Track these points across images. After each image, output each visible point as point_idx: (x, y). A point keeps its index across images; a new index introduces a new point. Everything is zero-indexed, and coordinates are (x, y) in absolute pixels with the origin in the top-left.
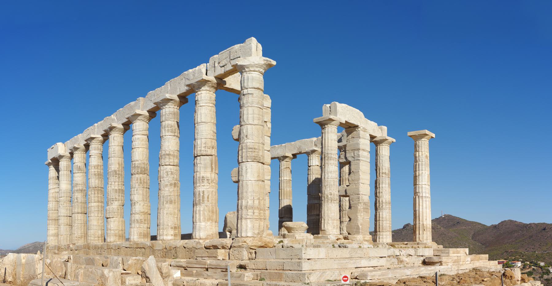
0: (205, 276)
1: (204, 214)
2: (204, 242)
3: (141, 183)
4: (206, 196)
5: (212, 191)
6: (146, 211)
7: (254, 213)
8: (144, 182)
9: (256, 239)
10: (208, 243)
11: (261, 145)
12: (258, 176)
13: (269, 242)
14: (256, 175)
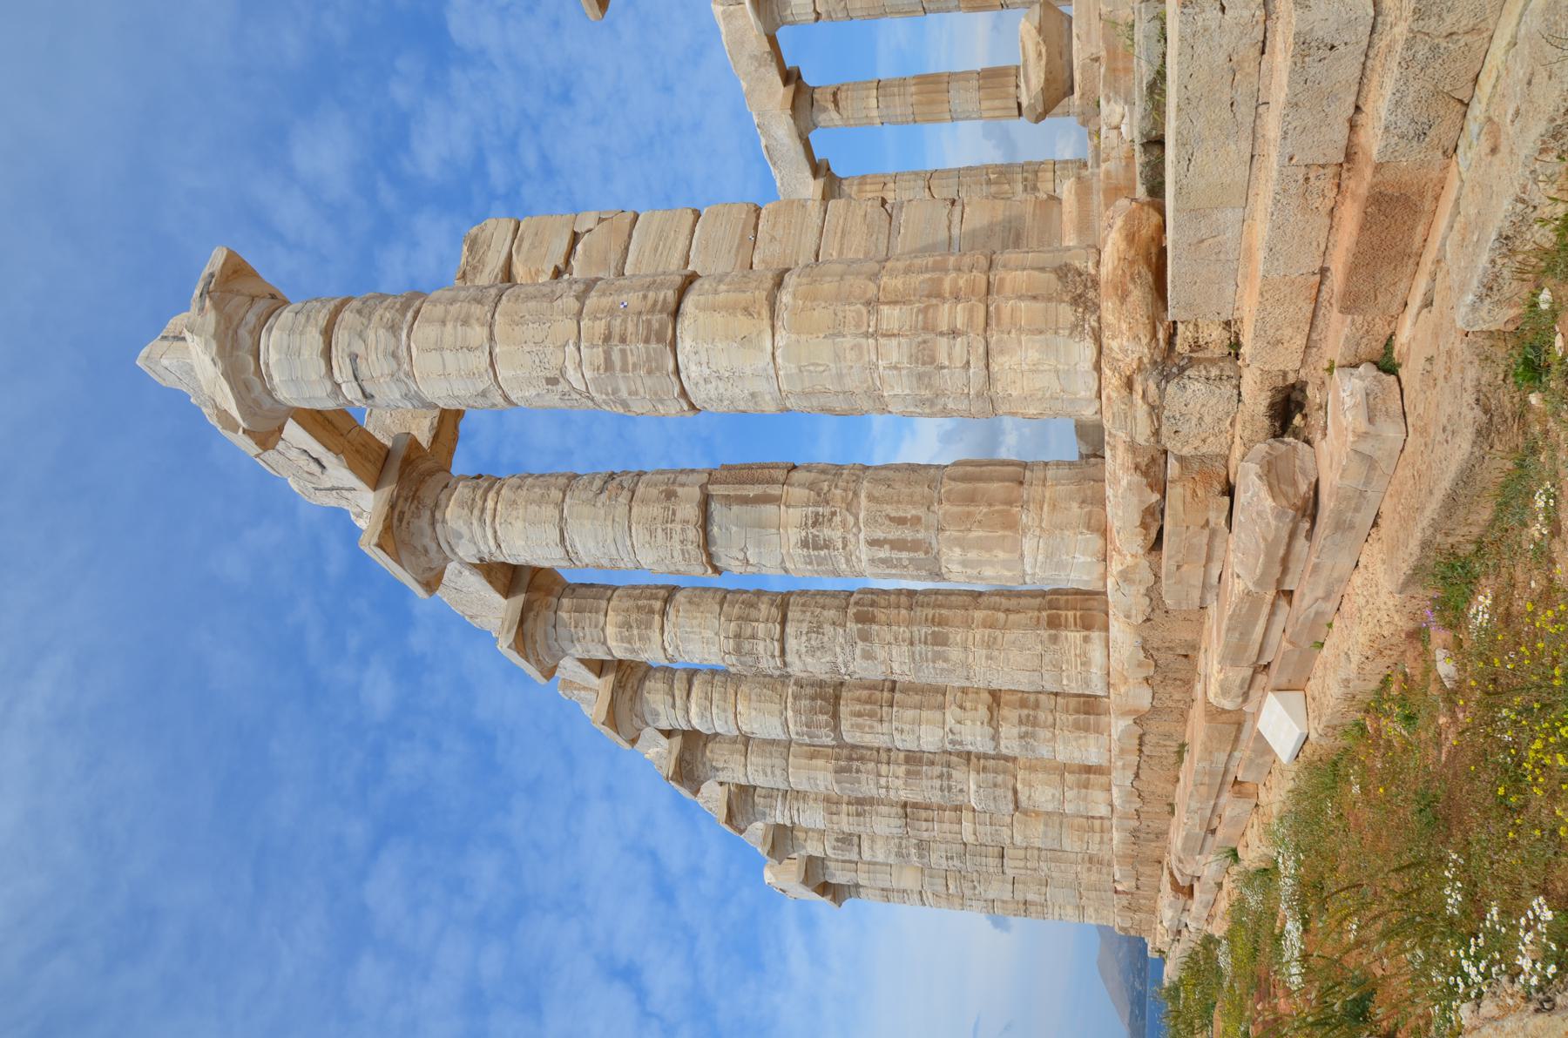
0: (1330, 607)
1: (980, 544)
2: (1119, 553)
3: (871, 715)
4: (896, 533)
5: (871, 498)
6: (986, 696)
7: (954, 333)
8: (869, 701)
9: (1109, 317)
10: (1128, 544)
11: (592, 301)
13: (1131, 238)
14: (742, 323)
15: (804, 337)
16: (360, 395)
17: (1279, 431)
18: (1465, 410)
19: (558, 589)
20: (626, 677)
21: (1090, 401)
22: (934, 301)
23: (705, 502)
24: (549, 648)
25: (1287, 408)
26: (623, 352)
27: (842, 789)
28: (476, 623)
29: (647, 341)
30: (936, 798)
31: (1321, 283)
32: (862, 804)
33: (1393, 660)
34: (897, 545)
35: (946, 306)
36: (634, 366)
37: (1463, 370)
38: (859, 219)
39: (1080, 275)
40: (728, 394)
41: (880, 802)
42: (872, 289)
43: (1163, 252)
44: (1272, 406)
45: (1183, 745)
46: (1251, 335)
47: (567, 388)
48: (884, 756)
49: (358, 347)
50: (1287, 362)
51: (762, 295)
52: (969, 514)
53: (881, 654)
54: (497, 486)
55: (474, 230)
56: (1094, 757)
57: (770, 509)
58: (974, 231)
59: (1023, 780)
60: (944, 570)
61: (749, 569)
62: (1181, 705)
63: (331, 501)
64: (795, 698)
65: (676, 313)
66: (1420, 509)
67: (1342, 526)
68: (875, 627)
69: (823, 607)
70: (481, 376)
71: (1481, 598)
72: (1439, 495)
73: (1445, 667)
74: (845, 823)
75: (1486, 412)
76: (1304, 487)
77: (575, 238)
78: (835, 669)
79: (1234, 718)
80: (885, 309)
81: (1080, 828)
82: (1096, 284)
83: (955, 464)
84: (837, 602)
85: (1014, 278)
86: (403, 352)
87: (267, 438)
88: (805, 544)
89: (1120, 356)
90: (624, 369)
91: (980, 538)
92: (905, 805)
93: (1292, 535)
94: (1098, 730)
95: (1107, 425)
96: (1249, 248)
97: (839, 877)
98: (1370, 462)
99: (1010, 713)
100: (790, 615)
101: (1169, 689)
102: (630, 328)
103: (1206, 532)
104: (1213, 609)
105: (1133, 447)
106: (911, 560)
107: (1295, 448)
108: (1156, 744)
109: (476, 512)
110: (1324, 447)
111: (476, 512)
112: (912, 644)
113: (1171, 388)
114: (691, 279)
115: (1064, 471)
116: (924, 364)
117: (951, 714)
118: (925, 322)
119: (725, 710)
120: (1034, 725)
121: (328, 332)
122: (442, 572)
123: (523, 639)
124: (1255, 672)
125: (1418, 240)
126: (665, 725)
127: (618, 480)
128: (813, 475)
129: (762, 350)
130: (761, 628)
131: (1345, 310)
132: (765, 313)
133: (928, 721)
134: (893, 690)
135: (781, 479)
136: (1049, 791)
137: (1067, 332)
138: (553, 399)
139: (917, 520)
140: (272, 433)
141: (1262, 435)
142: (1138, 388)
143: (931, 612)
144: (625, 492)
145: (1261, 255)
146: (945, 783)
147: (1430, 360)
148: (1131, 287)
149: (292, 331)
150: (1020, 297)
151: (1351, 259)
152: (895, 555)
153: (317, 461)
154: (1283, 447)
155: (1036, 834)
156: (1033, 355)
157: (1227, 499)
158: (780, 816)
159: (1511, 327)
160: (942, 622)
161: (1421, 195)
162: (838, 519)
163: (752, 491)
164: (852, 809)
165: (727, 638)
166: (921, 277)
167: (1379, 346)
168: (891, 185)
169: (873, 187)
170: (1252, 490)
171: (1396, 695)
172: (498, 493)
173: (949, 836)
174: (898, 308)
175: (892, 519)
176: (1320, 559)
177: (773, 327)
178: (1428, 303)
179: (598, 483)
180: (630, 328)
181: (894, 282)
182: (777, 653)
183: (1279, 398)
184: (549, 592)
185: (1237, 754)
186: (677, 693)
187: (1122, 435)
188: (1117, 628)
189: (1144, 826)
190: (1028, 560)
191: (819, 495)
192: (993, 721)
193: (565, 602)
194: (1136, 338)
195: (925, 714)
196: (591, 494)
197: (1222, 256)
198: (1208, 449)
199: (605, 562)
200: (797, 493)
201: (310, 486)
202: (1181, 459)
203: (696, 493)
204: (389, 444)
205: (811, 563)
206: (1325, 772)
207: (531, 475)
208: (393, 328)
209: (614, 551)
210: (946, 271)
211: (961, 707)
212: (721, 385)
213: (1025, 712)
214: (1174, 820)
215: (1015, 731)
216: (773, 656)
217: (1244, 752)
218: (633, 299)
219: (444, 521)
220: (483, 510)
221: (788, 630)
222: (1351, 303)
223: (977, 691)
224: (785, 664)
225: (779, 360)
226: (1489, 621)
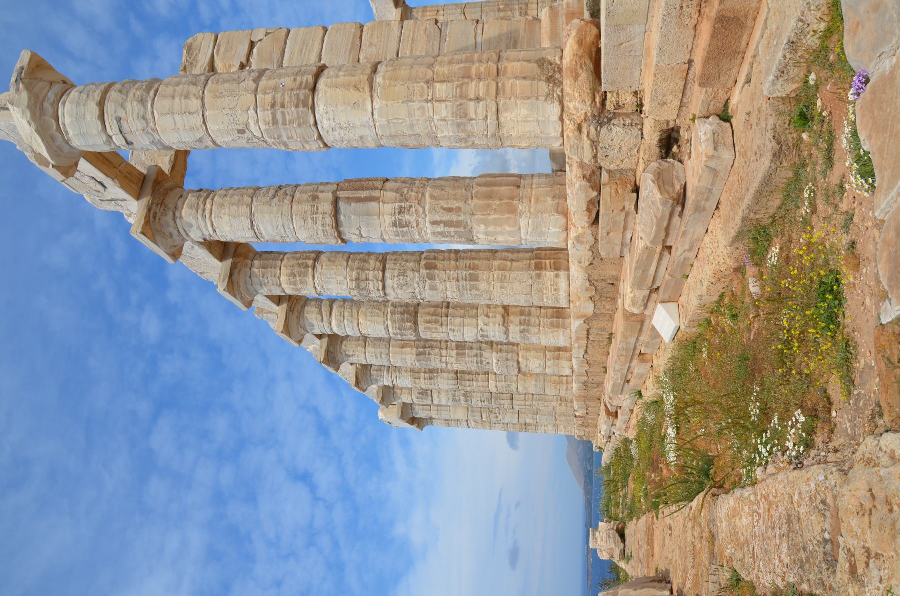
0: (692, 255)
1: (495, 223)
2: (575, 226)
3: (436, 322)
4: (447, 217)
5: (432, 197)
6: (501, 310)
7: (478, 99)
8: (435, 314)
9: (568, 89)
10: (580, 221)
11: (263, 83)
12: (356, 88)
13: (580, 43)
14: (354, 95)
15: (390, 103)
16: (124, 143)
17: (664, 156)
18: (767, 142)
19: (251, 255)
20: (294, 305)
21: (557, 138)
22: (466, 80)
23: (336, 202)
24: (248, 289)
25: (669, 142)
26: (283, 113)
27: (421, 365)
28: (204, 277)
29: (297, 106)
30: (474, 368)
31: (689, 69)
32: (432, 373)
33: (726, 284)
34: (448, 224)
35: (474, 83)
36: (290, 121)
37: (767, 120)
38: (422, 32)
39: (551, 64)
40: (346, 138)
41: (443, 371)
42: (430, 74)
43: (599, 51)
44: (661, 141)
45: (611, 334)
46: (649, 100)
47: (251, 136)
48: (444, 345)
49: (121, 113)
50: (670, 115)
51: (365, 78)
52: (489, 206)
53: (441, 287)
54: (212, 196)
55: (190, 41)
56: (562, 343)
57: (373, 205)
58: (490, 39)
59: (523, 356)
60: (475, 238)
61: (363, 240)
62: (610, 312)
63: (111, 207)
64: (392, 314)
65: (314, 89)
66: (742, 199)
67: (699, 209)
68: (437, 272)
69: (407, 261)
70: (198, 130)
71: (774, 249)
72: (752, 191)
73: (754, 288)
74: (424, 384)
75: (778, 144)
76: (678, 187)
77: (252, 45)
78: (414, 296)
79: (640, 319)
80: (438, 85)
81: (555, 382)
82: (560, 70)
83: (480, 177)
84: (414, 258)
85: (512, 67)
86: (149, 116)
87: (69, 170)
88: (395, 225)
89: (574, 112)
90: (284, 124)
91: (495, 219)
92: (457, 373)
93: (672, 215)
94: (564, 327)
95: (567, 153)
96: (649, 49)
97: (421, 414)
98: (715, 172)
99: (515, 319)
100: (387, 266)
101: (604, 303)
102: (287, 99)
103: (624, 214)
104: (627, 258)
105: (582, 165)
106: (456, 233)
107: (673, 165)
108: (597, 335)
109: (200, 211)
110: (689, 164)
111: (200, 211)
112: (458, 281)
113: (604, 131)
114: (322, 69)
115: (544, 180)
116: (461, 118)
117: (482, 320)
118: (461, 93)
119: (352, 322)
120: (528, 325)
121: (101, 104)
122: (182, 248)
123: (232, 286)
124: (651, 293)
125: (744, 44)
126: (318, 332)
127: (284, 190)
128: (398, 185)
129: (366, 110)
130: (371, 274)
131: (702, 85)
132: (367, 89)
133: (469, 325)
134: (448, 307)
135: (380, 187)
136: (538, 362)
137: (544, 98)
138: (242, 143)
139: (460, 209)
140: (71, 167)
141: (655, 158)
142: (585, 131)
143: (468, 262)
144: (288, 197)
145: (655, 52)
146: (479, 360)
147: (749, 114)
148: (581, 71)
149: (78, 104)
150: (517, 78)
151: (706, 55)
152: (447, 230)
153: (101, 183)
154: (667, 165)
155: (531, 386)
156: (524, 112)
157: (635, 195)
158: (386, 381)
159: (794, 95)
160: (475, 268)
161: (746, 17)
162: (413, 210)
163: (363, 194)
164: (427, 376)
165: (352, 280)
166: (459, 66)
167: (721, 106)
168: (442, 12)
169: (431, 14)
170: (650, 190)
171: (727, 304)
172: (213, 200)
173: (482, 389)
174: (444, 86)
175: (445, 209)
176: (687, 227)
177: (372, 97)
178: (748, 81)
179: (272, 192)
180: (287, 99)
181: (443, 69)
182: (381, 288)
183: (665, 136)
184: (246, 258)
185: (641, 338)
186: (324, 313)
187: (576, 158)
188: (575, 269)
189: (590, 380)
190: (523, 231)
191: (402, 196)
192: (505, 324)
193: (256, 262)
194: (584, 101)
195: (467, 321)
196: (268, 199)
197: (633, 53)
198: (627, 165)
199: (278, 238)
200: (390, 195)
201: (98, 199)
202: (609, 172)
203: (330, 196)
204: (145, 172)
205: (398, 236)
206: (688, 347)
207: (232, 189)
208: (143, 101)
209: (283, 232)
210: (473, 63)
211: (487, 316)
212: (342, 132)
213: (523, 318)
214: (607, 376)
215: (518, 329)
216: (379, 290)
217: (644, 338)
218: (288, 82)
219: (181, 218)
220: (204, 210)
221: (387, 275)
222: (706, 81)
223: (496, 307)
224: (386, 295)
225: (376, 117)
226: (778, 261)
